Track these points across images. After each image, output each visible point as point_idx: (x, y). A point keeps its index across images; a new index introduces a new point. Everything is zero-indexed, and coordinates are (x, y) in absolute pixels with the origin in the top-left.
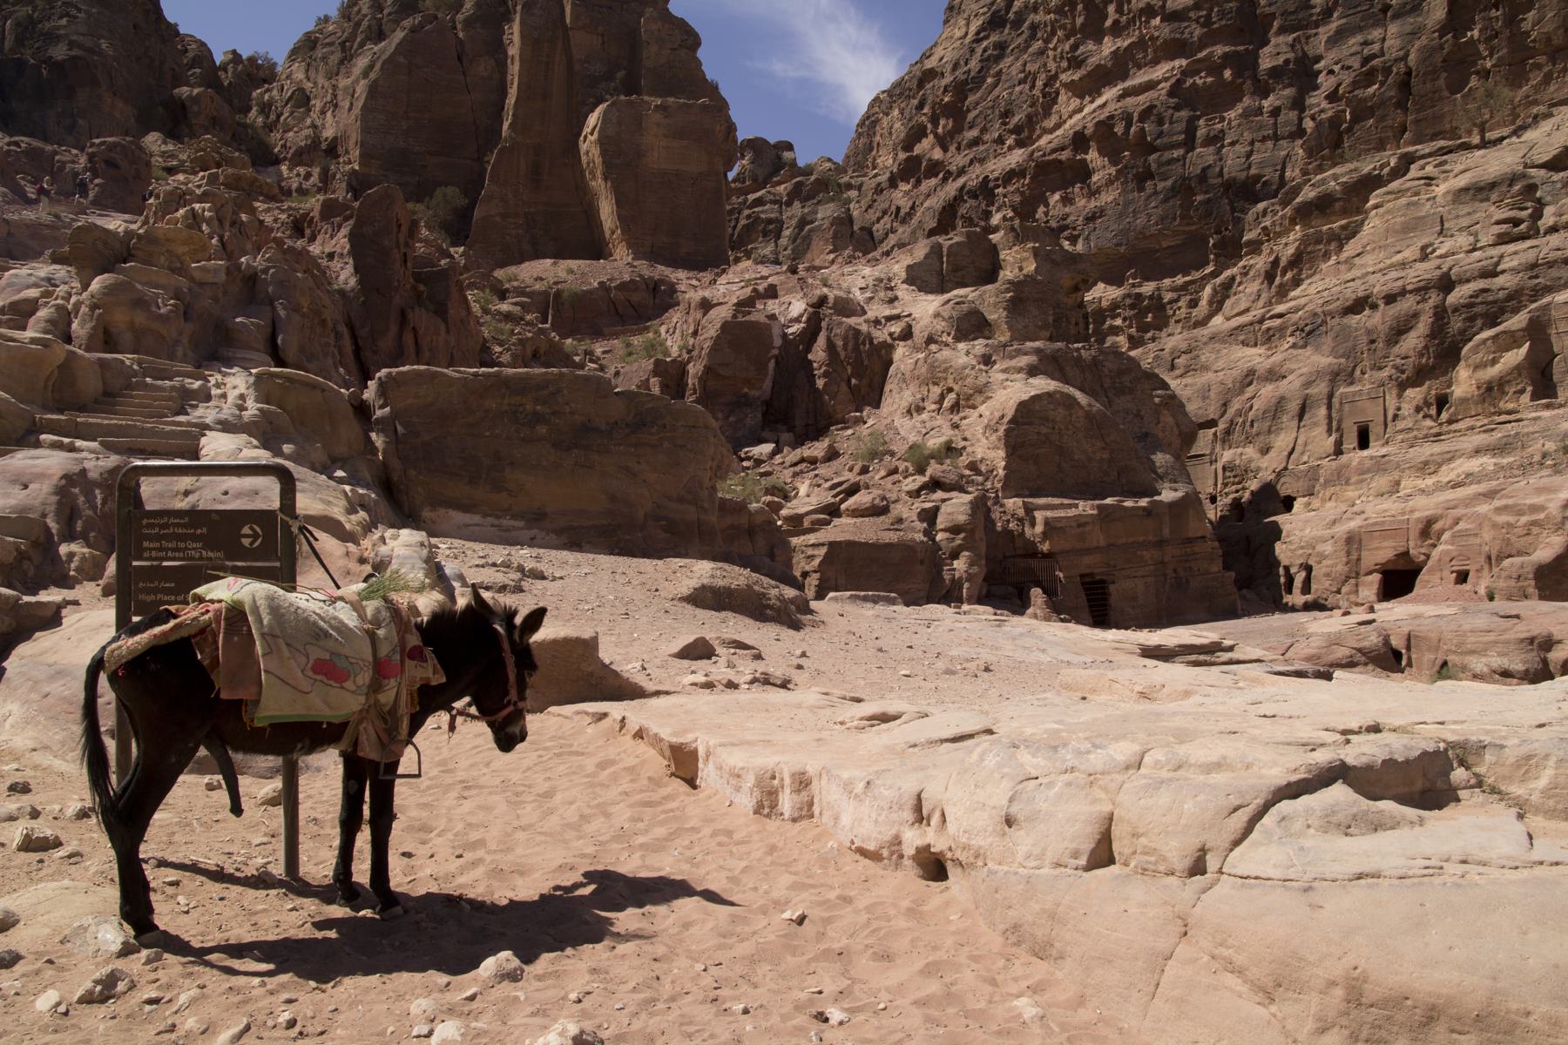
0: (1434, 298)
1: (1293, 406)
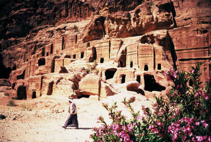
0: (35, 44)
1: (21, 56)
